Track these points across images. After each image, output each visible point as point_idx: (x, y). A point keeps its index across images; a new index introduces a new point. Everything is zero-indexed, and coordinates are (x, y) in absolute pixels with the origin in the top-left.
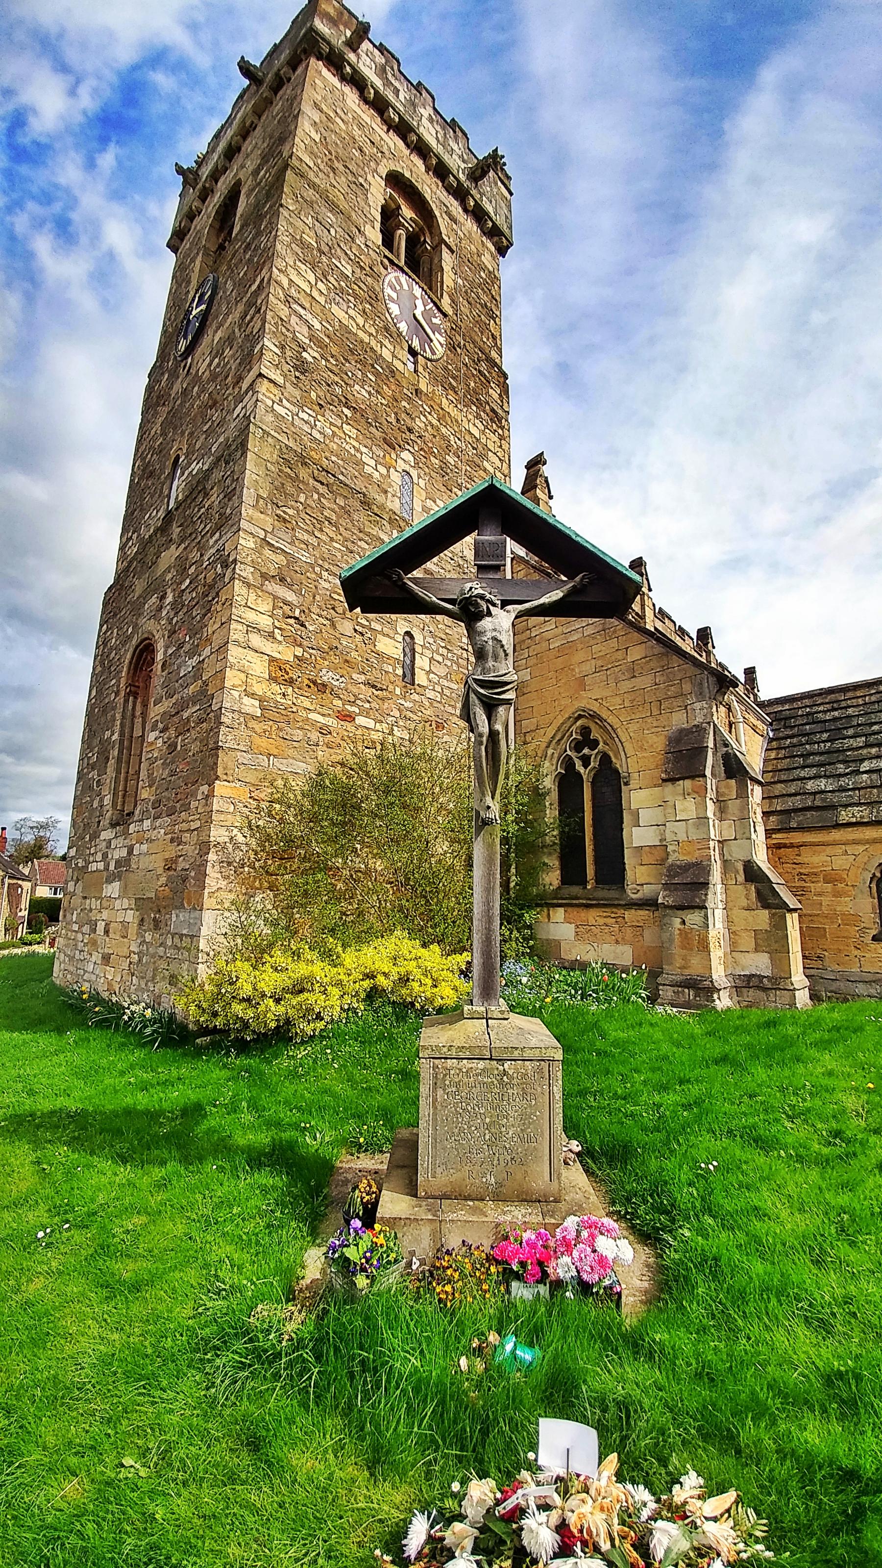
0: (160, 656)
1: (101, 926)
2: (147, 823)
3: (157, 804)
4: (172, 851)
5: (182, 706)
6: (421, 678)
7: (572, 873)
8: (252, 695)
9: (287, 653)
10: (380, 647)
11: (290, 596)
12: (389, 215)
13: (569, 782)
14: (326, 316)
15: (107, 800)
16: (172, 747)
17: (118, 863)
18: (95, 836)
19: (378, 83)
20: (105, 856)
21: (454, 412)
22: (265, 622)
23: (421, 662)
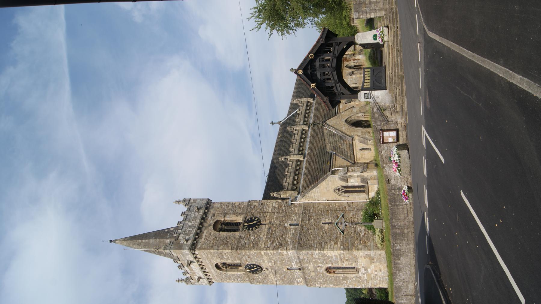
0: (330, 265)
1: (376, 273)
2: (359, 264)
3: (356, 262)
4: (363, 258)
5: (341, 258)
6: (330, 221)
7: (363, 191)
9: (333, 243)
11: (323, 243)
12: (221, 230)
13: (346, 192)
15: (354, 275)
16: (347, 260)
17: (365, 270)
18: (360, 278)
19: (192, 235)
20: (364, 274)
21: (269, 215)
22: (329, 246)
23: (327, 221)
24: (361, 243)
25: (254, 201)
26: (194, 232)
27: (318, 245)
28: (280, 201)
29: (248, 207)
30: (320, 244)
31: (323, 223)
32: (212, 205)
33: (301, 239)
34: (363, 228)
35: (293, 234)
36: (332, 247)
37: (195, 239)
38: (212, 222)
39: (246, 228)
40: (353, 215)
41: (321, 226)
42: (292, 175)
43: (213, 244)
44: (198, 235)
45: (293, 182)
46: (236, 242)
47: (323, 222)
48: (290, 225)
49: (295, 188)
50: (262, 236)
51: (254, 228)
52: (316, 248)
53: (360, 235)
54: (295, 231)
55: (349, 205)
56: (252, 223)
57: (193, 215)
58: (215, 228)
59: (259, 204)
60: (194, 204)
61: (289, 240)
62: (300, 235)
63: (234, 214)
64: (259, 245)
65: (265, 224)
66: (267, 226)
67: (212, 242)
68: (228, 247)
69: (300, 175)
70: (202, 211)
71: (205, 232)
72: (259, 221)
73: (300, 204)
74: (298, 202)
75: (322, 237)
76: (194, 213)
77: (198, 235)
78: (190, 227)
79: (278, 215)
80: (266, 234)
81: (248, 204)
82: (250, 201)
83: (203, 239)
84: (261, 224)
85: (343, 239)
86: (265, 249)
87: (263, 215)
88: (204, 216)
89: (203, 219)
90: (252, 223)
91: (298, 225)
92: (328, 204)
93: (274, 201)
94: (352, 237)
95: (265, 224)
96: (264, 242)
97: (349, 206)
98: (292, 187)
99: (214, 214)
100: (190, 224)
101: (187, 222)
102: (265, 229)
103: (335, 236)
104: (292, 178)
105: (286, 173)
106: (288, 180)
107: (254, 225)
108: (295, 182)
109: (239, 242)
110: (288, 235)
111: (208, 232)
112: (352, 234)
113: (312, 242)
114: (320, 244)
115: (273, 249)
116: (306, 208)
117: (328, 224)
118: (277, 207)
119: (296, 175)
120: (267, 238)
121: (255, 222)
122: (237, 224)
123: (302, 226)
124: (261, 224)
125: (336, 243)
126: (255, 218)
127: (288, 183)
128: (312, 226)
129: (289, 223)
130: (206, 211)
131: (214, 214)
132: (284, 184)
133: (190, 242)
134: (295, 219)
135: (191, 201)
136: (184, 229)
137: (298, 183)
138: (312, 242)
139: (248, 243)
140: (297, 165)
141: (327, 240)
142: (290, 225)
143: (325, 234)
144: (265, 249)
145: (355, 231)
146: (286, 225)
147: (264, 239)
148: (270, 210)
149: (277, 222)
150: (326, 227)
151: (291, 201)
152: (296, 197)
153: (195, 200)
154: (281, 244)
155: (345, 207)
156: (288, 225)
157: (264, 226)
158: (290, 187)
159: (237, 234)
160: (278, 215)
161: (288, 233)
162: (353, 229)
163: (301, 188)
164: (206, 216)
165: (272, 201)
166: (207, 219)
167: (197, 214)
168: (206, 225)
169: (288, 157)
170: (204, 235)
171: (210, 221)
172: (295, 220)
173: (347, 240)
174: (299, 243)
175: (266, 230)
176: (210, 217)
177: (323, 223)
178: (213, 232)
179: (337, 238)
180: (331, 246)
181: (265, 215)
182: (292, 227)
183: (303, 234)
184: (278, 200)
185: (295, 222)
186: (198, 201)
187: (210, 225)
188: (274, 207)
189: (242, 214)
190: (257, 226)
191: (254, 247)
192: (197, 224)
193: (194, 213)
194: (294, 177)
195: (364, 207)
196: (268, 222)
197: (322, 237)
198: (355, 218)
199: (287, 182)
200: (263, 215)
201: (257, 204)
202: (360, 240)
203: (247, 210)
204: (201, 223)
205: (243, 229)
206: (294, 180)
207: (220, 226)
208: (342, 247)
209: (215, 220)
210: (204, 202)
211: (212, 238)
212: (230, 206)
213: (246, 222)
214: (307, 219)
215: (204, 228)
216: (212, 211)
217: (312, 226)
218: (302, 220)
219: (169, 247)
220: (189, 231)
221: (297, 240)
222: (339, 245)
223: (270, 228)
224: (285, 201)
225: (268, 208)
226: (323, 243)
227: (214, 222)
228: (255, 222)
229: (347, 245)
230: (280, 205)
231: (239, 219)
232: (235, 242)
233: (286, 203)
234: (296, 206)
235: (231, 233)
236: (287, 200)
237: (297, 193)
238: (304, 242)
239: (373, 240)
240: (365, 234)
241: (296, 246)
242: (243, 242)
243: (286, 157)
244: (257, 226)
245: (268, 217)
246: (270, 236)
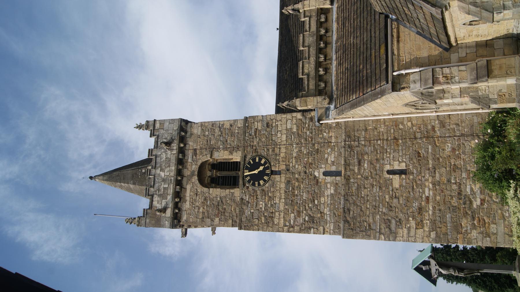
6: (403, 166)
8: (430, 234)
9: (413, 223)
10: (397, 186)
11: (393, 221)
14: (286, 212)
19: (169, 197)
21: (283, 150)
22: (405, 231)
23: (397, 166)
24: (474, 227)
25: (253, 117)
26: (171, 191)
27: (383, 226)
28: (299, 116)
29: (245, 133)
30: (388, 222)
31: (389, 172)
32: (189, 129)
33: (349, 210)
34: (478, 185)
35: (332, 194)
36: (412, 233)
37: (176, 206)
38: (195, 168)
39: (249, 181)
40: (453, 150)
41: (386, 180)
42: (313, 51)
43: (203, 213)
44: (178, 195)
45: (317, 71)
46: (237, 211)
47: (388, 167)
48: (326, 174)
49: (323, 85)
50: (277, 201)
51: (262, 182)
52: (380, 233)
53: (471, 202)
54: (335, 190)
55: (442, 122)
56: (256, 172)
57: (164, 156)
58: (201, 181)
59: (263, 126)
60: (162, 131)
61: (326, 211)
62: (346, 200)
63: (225, 149)
64: (276, 221)
65: (279, 173)
66: (283, 176)
67: (201, 210)
68: (226, 220)
69: (328, 50)
70: (175, 146)
71: (188, 187)
72: (268, 165)
73: (338, 123)
74: (333, 121)
75: (390, 208)
76: (165, 152)
77: (178, 195)
78: (164, 180)
79: (300, 151)
80: (283, 195)
81: (245, 126)
82: (246, 119)
83: (188, 203)
84: (273, 173)
85: (434, 213)
86: (286, 228)
87: (273, 151)
88: (181, 157)
89: (181, 162)
90: (256, 172)
91: (337, 174)
92: (396, 123)
93: (289, 116)
94: (455, 209)
95: (279, 173)
96: (282, 214)
97: (443, 125)
98: (317, 85)
99: (195, 150)
100: (162, 174)
101: (158, 171)
102: (280, 181)
103: (416, 205)
104: (312, 59)
105: (301, 48)
106: (306, 66)
107: (261, 175)
108: (322, 72)
109: (242, 212)
110: (322, 199)
111: (192, 187)
112: (454, 202)
113: (371, 220)
114: (388, 222)
115: (300, 231)
116: (350, 132)
117: (401, 172)
118: (295, 130)
119: (320, 51)
120: (286, 204)
121: (261, 168)
122: (235, 166)
123: (347, 179)
124: (273, 173)
125: (420, 225)
126: (260, 160)
127: (308, 75)
128: (367, 178)
129: (322, 170)
130: (182, 145)
131: (195, 150)
132: (301, 76)
133: (169, 213)
134: (332, 158)
135: (157, 126)
136: (157, 185)
137: (326, 70)
138: (371, 220)
139: (256, 215)
140: (320, 24)
141: (401, 216)
142: (326, 174)
143: (395, 201)
144: (286, 228)
145: (460, 194)
146: (316, 174)
147: (282, 208)
148: (284, 137)
149: (300, 168)
150: (396, 180)
151: (319, 120)
152: (328, 109)
153: (162, 122)
154: (312, 219)
155: (433, 128)
156: (322, 176)
157: (277, 177)
158: (312, 86)
159: (237, 192)
160: (300, 151)
161: (322, 194)
162: (454, 187)
163: (334, 88)
164: (184, 156)
165: (284, 116)
166: (187, 162)
167: (169, 152)
168: (187, 172)
169: (299, 6)
170: (188, 193)
171: (192, 167)
172: (333, 163)
173: (443, 217)
174: (346, 221)
175: (283, 186)
176: (190, 154)
177: (389, 172)
178: (200, 189)
179: (420, 209)
180: (409, 229)
181: (277, 151)
182: (329, 179)
183: (350, 199)
184: (294, 114)
185: (333, 168)
186: (167, 124)
187: (192, 174)
188: (289, 131)
189: (238, 148)
190: (266, 178)
191: (267, 223)
192: (172, 174)
193: (165, 152)
194: (318, 58)
195: (477, 129)
196: (284, 167)
197: (390, 208)
198: (459, 157)
199: (306, 71)
200: (273, 151)
201: (259, 126)
202: (473, 218)
203: (244, 139)
204: (179, 173)
205: (244, 185)
206: (318, 64)
207: (209, 174)
208: (433, 235)
209: (199, 163)
210: (176, 127)
211: (200, 200)
212: (217, 130)
213: (247, 168)
214: (356, 161)
215: (185, 179)
216: (191, 144)
217: (367, 178)
218: (347, 165)
219: (143, 222)
220: (164, 188)
221: (342, 210)
222: (427, 229)
223: (288, 182)
224: (309, 115)
225: (279, 135)
226: (393, 221)
227: (197, 167)
228: (261, 168)
229: (444, 229)
230: (300, 125)
231: (237, 157)
232: (235, 209)
233: (311, 119)
234: (329, 127)
235: (228, 191)
236: (313, 114)
237: (327, 100)
238: (354, 218)
239: (504, 218)
240: (483, 201)
241: (341, 225)
242: (247, 212)
243: (296, 6)
244: (266, 178)
245: (282, 155)
246: (291, 200)
